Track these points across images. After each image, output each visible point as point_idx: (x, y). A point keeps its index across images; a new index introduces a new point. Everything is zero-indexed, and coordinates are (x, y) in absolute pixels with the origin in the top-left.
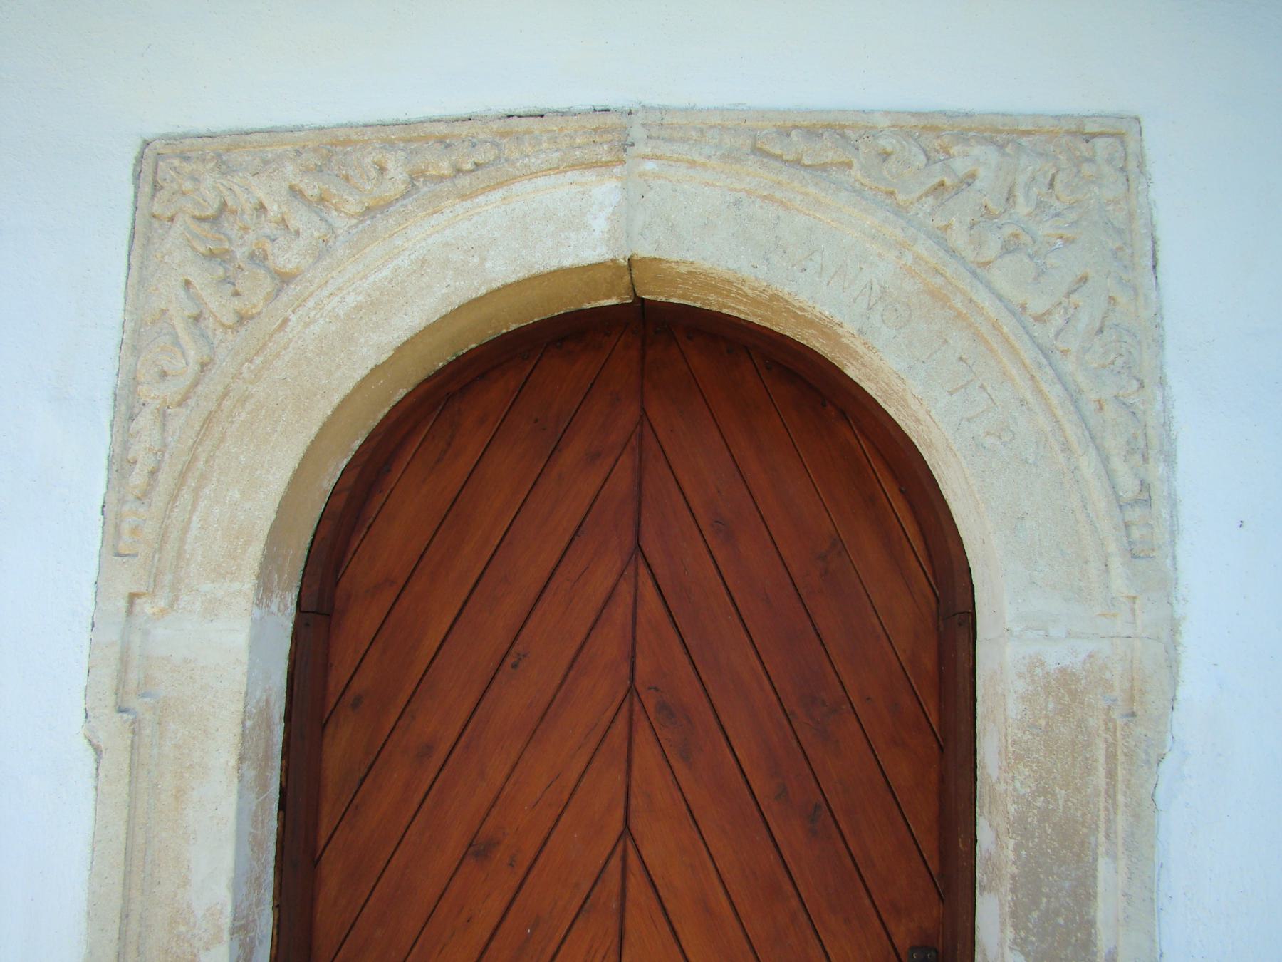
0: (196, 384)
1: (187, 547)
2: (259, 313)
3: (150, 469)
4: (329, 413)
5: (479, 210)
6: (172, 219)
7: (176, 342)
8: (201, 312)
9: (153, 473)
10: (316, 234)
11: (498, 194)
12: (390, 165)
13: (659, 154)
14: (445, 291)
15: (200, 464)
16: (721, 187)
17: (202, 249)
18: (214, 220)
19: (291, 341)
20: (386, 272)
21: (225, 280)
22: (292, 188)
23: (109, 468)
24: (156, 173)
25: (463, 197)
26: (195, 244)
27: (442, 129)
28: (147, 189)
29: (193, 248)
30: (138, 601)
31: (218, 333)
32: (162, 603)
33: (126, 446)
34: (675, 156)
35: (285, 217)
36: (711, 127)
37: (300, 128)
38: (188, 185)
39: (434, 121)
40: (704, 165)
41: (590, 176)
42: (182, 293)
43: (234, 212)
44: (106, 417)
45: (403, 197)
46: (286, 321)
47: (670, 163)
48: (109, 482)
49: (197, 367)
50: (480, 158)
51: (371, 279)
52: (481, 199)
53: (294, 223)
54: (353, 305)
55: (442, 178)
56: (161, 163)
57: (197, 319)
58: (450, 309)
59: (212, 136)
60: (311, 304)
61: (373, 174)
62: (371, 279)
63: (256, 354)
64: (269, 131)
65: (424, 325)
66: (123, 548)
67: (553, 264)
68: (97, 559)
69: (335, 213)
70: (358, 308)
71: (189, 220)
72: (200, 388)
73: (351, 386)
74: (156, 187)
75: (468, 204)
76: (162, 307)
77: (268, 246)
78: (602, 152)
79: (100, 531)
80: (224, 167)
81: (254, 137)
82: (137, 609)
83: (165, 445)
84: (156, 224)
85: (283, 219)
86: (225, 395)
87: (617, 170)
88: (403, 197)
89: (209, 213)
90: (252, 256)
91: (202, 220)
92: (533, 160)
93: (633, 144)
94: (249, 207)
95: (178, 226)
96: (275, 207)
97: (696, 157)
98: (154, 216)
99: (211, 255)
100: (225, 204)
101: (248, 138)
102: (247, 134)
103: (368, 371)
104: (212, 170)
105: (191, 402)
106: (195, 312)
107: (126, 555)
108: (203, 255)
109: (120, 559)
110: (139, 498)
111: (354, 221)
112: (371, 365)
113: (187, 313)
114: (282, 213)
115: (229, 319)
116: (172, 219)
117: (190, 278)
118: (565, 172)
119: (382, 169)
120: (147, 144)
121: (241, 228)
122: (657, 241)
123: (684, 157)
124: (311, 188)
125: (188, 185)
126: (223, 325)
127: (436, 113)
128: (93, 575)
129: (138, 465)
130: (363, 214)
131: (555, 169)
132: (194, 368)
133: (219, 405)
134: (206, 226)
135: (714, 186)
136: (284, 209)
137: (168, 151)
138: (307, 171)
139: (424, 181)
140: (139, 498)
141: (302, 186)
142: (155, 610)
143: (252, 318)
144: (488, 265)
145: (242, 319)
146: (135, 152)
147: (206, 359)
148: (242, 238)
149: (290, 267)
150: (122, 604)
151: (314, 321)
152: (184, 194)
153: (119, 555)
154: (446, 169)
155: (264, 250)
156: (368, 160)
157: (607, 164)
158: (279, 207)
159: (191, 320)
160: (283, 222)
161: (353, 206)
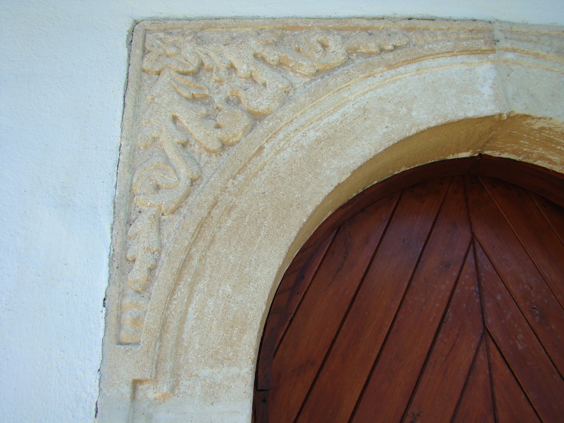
0: (187, 195)
1: (185, 336)
2: (238, 142)
3: (149, 266)
4: (305, 220)
5: (400, 77)
6: (159, 73)
7: (167, 161)
8: (188, 140)
9: (151, 270)
10: (280, 86)
11: (413, 67)
12: (331, 43)
13: (516, 48)
14: (385, 130)
15: (195, 262)
16: (556, 71)
17: (186, 94)
18: (195, 74)
19: (265, 164)
20: (336, 116)
21: (207, 117)
22: (255, 56)
23: (110, 265)
24: (144, 41)
25: (390, 67)
26: (180, 91)
27: (365, 23)
28: (138, 52)
29: (179, 94)
30: (140, 387)
31: (203, 156)
32: (165, 389)
33: (125, 247)
34: (526, 50)
35: (253, 74)
36: (544, 35)
37: (258, 18)
38: (172, 50)
39: (358, 18)
40: (544, 57)
41: (474, 59)
42: (171, 125)
43: (210, 70)
44: (106, 221)
45: (344, 64)
46: (261, 148)
47: (522, 55)
48: (110, 276)
49: (188, 182)
50: (397, 43)
51: (326, 120)
52: (402, 69)
53: (261, 78)
54: (314, 139)
55: (370, 54)
56: (148, 35)
57: (184, 145)
58: (391, 143)
59: (190, 20)
60: (281, 136)
61: (319, 48)
62: (326, 120)
63: (239, 173)
64: (234, 19)
65: (373, 154)
66: (124, 336)
67: (461, 115)
68: (101, 347)
69: (291, 74)
70: (318, 141)
71: (175, 75)
72: (190, 199)
73: (321, 199)
74: (145, 52)
75: (392, 72)
76: (155, 135)
77: (242, 94)
78: (481, 44)
79: (103, 321)
80: (199, 40)
81: (222, 21)
82: (140, 394)
83: (161, 246)
84: (145, 77)
85: (251, 76)
86: (215, 205)
87: (491, 56)
88: (344, 64)
89: (191, 69)
90: (228, 100)
91: (185, 74)
92: (435, 46)
93: (498, 41)
94: (223, 67)
95: (165, 78)
96: (245, 67)
97: (540, 52)
98: (144, 71)
99: (193, 99)
100: (202, 64)
101: (218, 21)
102: (216, 19)
103: (332, 188)
104: (191, 41)
105: (184, 210)
106: (184, 139)
107: (128, 344)
108: (187, 98)
109: (122, 347)
110: (138, 292)
111: (307, 80)
112: (335, 184)
113: (176, 140)
114: (251, 72)
115: (215, 145)
116: (159, 73)
117: (177, 114)
118: (457, 55)
119: (324, 46)
120: (136, 23)
121: (216, 81)
122: (525, 103)
123: (532, 51)
124: (273, 56)
125: (172, 50)
126: (208, 150)
127: (359, 14)
128: (97, 363)
129: (137, 263)
130: (314, 75)
131: (451, 53)
132: (184, 183)
133: (209, 213)
134: (189, 78)
135: (553, 71)
136: (252, 68)
137: (154, 28)
138: (267, 44)
139: (357, 56)
140: (138, 292)
141: (264, 54)
142: (157, 395)
143: (232, 145)
144: (414, 114)
145: (224, 146)
146: (128, 27)
147: (195, 176)
148: (217, 88)
149: (262, 108)
150: (126, 390)
151: (283, 149)
152: (168, 56)
153: (120, 343)
154: (373, 48)
155: (237, 96)
156: (314, 39)
157: (484, 52)
158: (248, 67)
159: (180, 146)
160: (251, 78)
161: (307, 68)
